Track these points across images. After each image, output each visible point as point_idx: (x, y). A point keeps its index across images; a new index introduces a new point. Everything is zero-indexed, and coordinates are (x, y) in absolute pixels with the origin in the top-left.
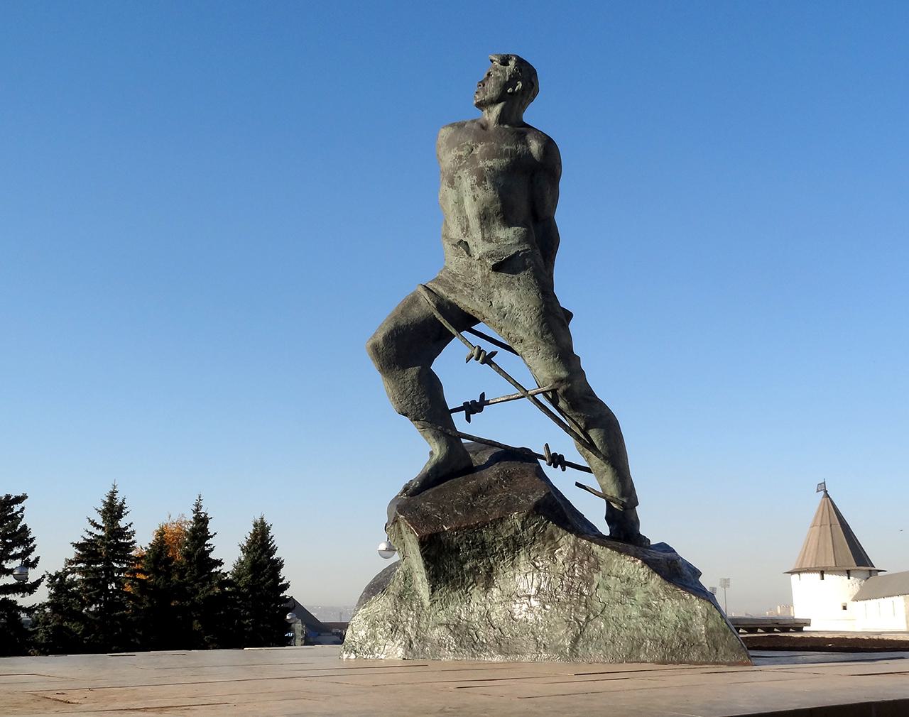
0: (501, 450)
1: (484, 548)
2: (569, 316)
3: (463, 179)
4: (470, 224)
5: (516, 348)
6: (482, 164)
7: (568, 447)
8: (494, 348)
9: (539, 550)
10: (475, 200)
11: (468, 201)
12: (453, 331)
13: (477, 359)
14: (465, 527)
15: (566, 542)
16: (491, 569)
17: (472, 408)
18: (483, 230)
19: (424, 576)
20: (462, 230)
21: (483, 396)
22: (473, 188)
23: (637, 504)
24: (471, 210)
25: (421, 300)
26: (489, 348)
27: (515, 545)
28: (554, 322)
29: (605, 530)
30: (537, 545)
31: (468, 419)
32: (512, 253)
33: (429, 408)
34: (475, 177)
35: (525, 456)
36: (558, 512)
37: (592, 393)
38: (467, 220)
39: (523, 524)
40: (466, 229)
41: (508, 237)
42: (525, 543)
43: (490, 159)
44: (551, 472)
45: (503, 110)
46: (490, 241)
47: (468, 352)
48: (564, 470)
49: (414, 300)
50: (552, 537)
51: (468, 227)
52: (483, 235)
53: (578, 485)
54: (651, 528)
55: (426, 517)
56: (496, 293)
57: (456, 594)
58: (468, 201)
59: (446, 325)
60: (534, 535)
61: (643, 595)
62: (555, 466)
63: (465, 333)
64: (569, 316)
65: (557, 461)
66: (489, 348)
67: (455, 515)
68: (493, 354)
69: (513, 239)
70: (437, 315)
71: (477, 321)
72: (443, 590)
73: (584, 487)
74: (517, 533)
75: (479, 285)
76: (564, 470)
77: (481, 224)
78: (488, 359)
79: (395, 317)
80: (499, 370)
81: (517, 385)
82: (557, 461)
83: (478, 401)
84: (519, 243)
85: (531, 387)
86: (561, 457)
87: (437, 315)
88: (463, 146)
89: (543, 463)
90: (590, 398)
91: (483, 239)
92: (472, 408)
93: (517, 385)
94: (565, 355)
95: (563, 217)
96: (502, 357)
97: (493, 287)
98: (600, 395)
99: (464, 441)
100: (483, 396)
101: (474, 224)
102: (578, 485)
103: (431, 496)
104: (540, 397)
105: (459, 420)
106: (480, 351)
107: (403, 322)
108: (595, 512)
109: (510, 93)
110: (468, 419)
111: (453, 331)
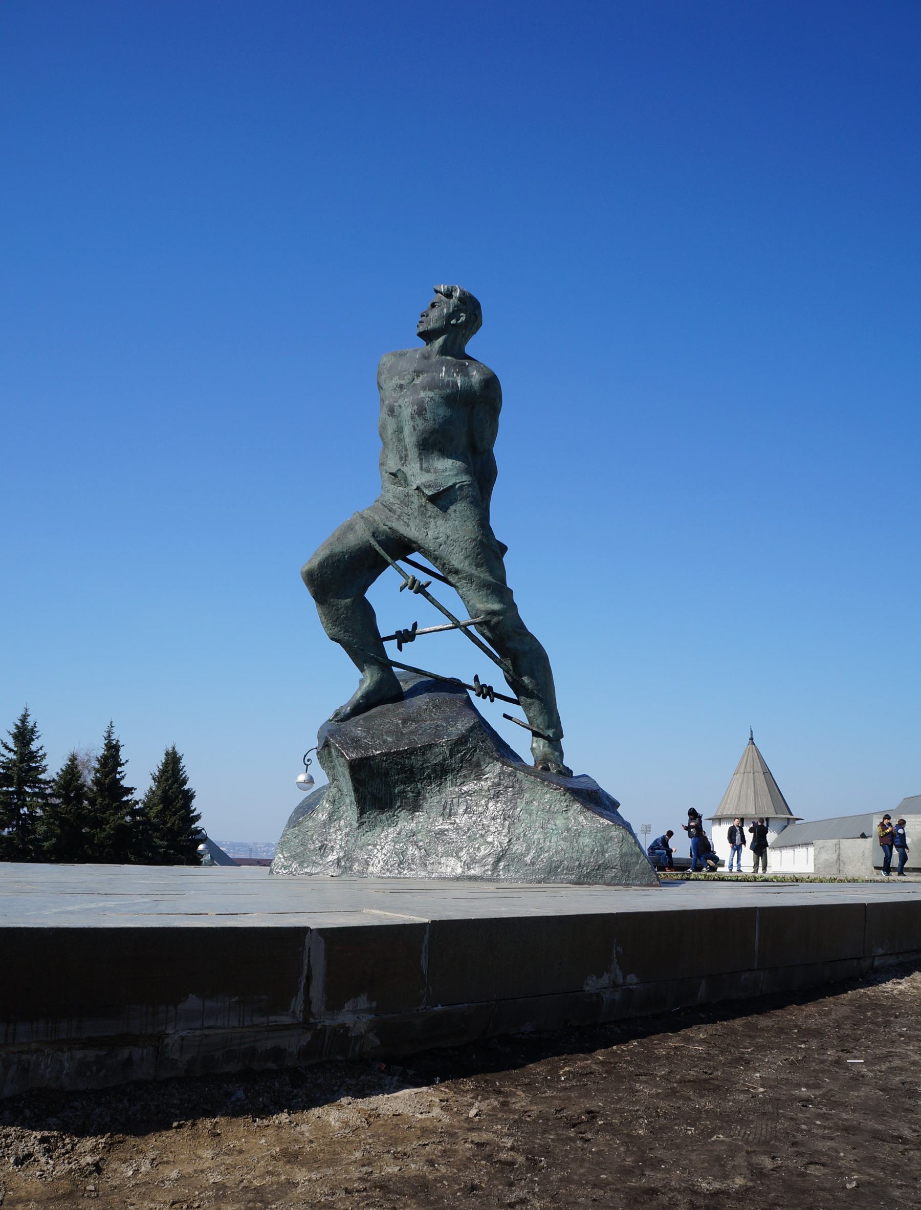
0: (429, 679)
1: (412, 772)
2: (503, 549)
3: (403, 408)
4: (409, 453)
5: (450, 578)
6: (422, 394)
7: (495, 676)
8: (430, 578)
9: (465, 776)
10: (415, 429)
11: (407, 430)
12: (389, 559)
13: (411, 588)
14: (394, 752)
15: (493, 770)
16: (419, 793)
17: (405, 637)
18: (421, 460)
19: (353, 799)
20: (401, 459)
21: (415, 626)
22: (412, 418)
23: (562, 736)
24: (410, 439)
25: (357, 527)
26: (423, 578)
27: (441, 773)
28: (490, 552)
29: (529, 760)
30: (464, 772)
31: (400, 648)
32: (450, 484)
33: (360, 636)
34: (415, 407)
35: (454, 686)
36: (485, 743)
37: (523, 626)
38: (406, 450)
39: (451, 750)
40: (404, 459)
41: (447, 471)
42: (453, 770)
43: (431, 389)
44: (480, 703)
45: (445, 341)
46: (428, 471)
47: (403, 581)
48: (492, 701)
49: (350, 528)
50: (478, 765)
51: (406, 456)
52: (421, 464)
53: (505, 716)
54: (578, 758)
55: (356, 742)
56: (432, 525)
57: (383, 817)
58: (407, 430)
59: (382, 552)
60: (462, 762)
61: (564, 821)
62: (484, 697)
63: (400, 563)
64: (503, 549)
65: (487, 692)
66: (423, 578)
67: (385, 741)
68: (429, 583)
69: (451, 470)
70: (373, 542)
71: (412, 551)
72: (372, 815)
73: (510, 718)
74: (444, 760)
75: (416, 514)
76: (492, 701)
77: (420, 454)
78: (421, 589)
79: (331, 544)
80: (433, 601)
81: (449, 615)
82: (487, 692)
83: (410, 630)
84: (457, 475)
85: (464, 617)
86: (490, 688)
87: (373, 542)
88: (405, 375)
89: (472, 694)
90: (521, 631)
91: (421, 468)
92: (405, 637)
93: (449, 615)
94: (499, 589)
95: (498, 450)
96: (437, 588)
97: (430, 517)
98: (530, 628)
99: (395, 669)
100: (415, 626)
101: (413, 453)
102: (505, 716)
103: (361, 722)
104: (472, 628)
105: (391, 649)
106: (414, 581)
107: (338, 549)
108: (522, 742)
109: (453, 325)
110: (400, 648)
111: (389, 559)
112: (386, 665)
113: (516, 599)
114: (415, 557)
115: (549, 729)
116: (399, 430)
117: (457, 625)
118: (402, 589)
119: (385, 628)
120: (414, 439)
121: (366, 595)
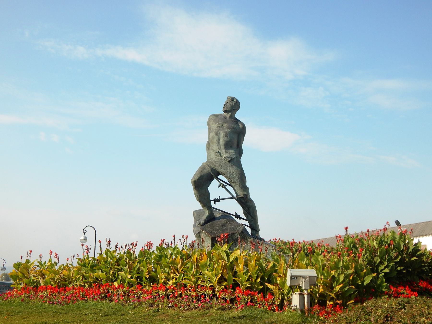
5: (233, 184)
6: (226, 130)
11: (221, 140)
17: (216, 201)
21: (220, 197)
24: (222, 142)
25: (206, 168)
31: (215, 203)
40: (220, 148)
46: (227, 153)
50: (247, 239)
56: (228, 168)
58: (221, 140)
66: (225, 184)
71: (219, 174)
78: (224, 187)
82: (238, 217)
85: (235, 196)
92: (216, 201)
94: (245, 188)
96: (228, 187)
100: (220, 197)
101: (222, 147)
107: (202, 174)
110: (215, 203)
112: (210, 208)
113: (250, 191)
114: (221, 177)
115: (255, 228)
116: (219, 140)
117: (233, 197)
118: (219, 187)
119: (212, 198)
120: (224, 143)
121: (209, 189)
